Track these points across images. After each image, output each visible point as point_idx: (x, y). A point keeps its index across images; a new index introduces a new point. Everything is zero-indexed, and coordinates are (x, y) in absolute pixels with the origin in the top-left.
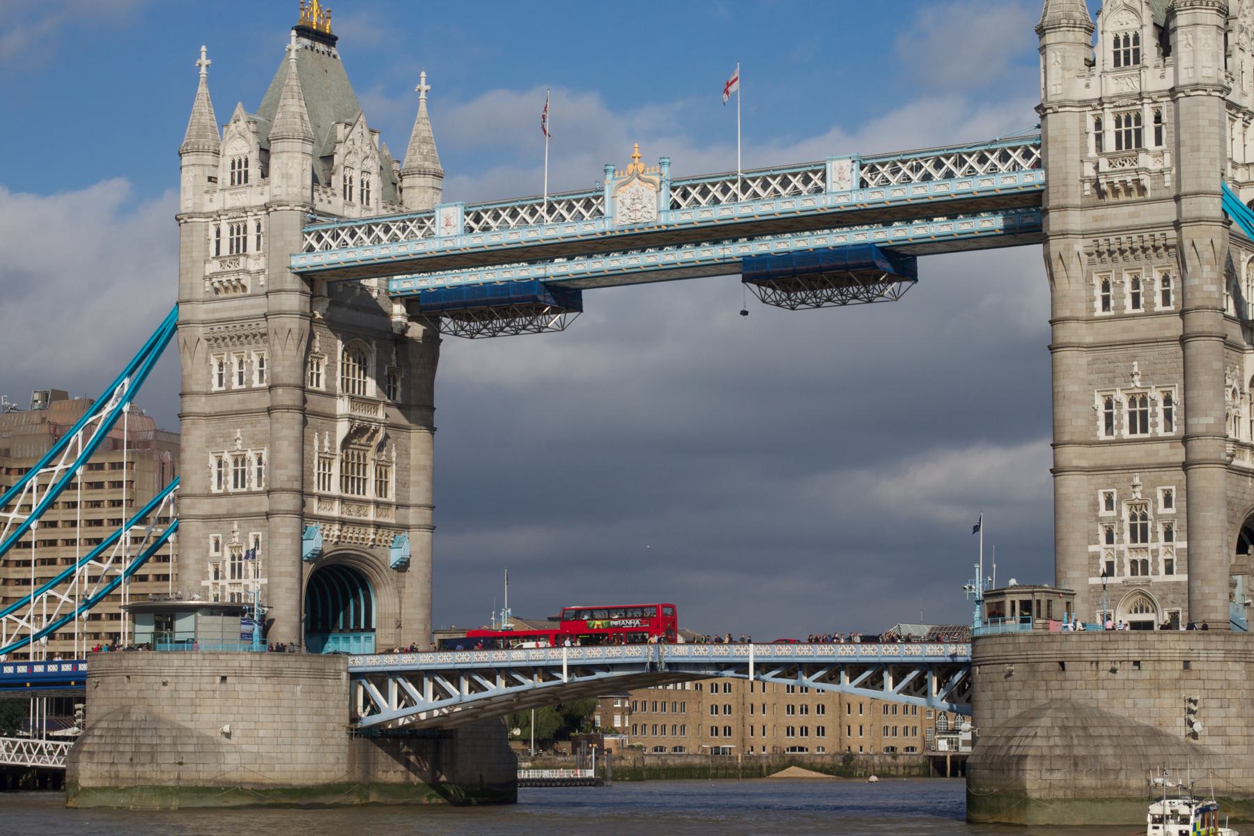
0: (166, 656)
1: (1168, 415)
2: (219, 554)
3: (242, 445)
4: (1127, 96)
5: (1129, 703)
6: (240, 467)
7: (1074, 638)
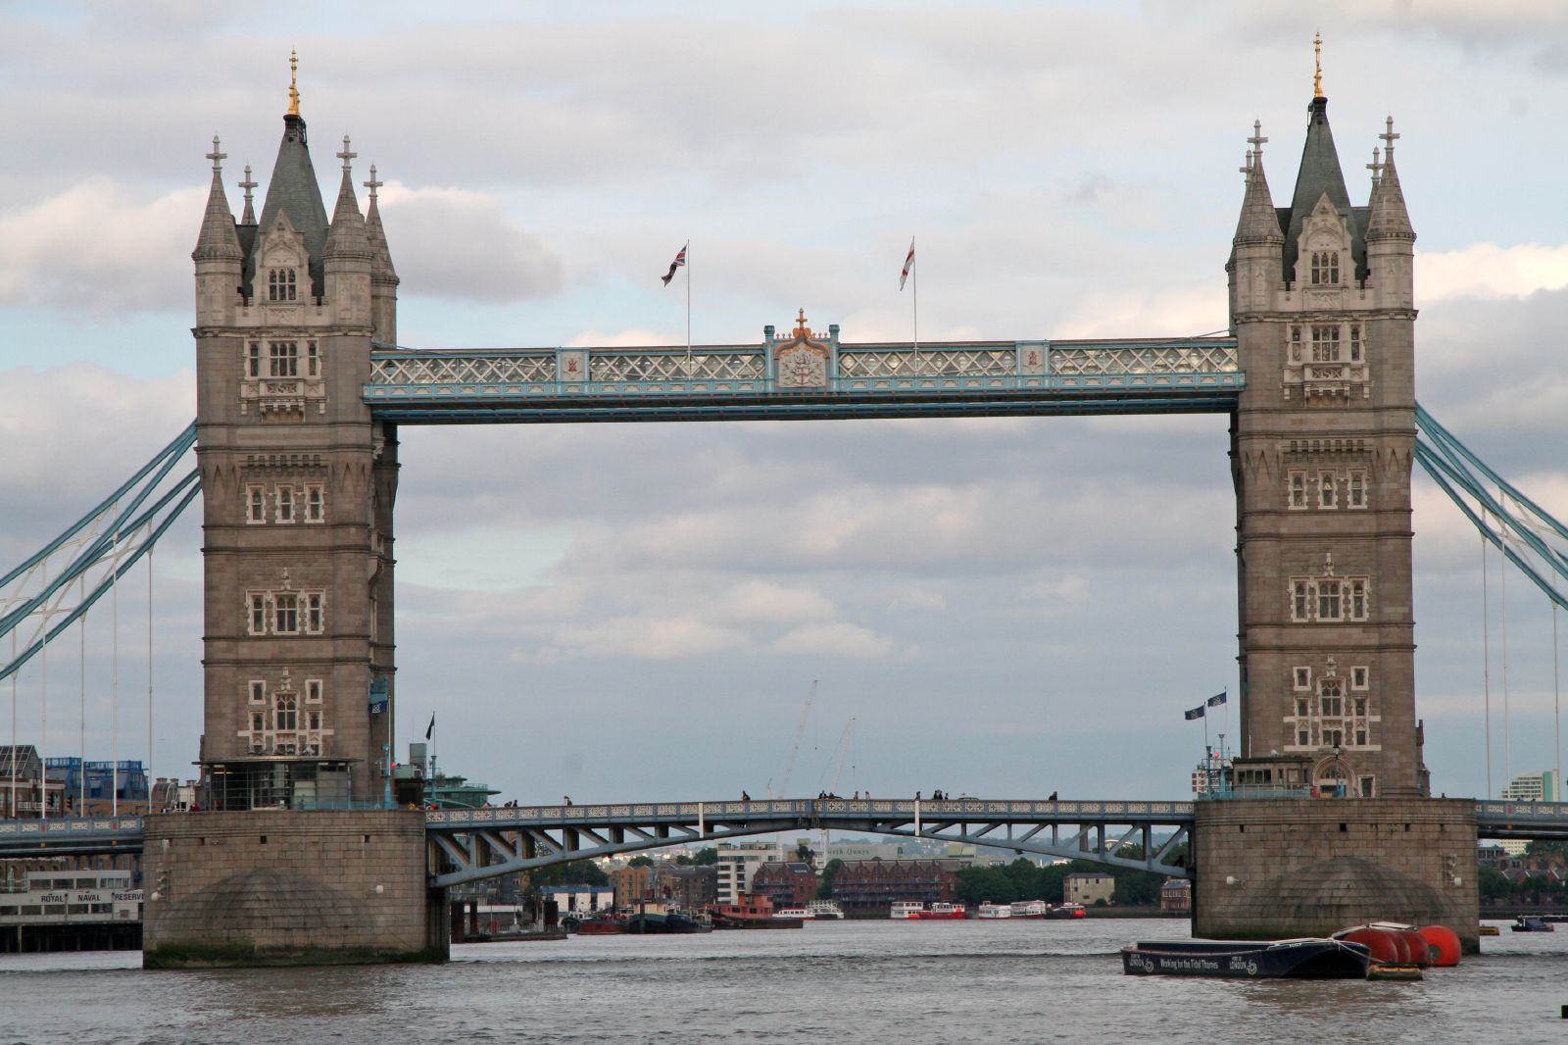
0: (312, 815)
1: (1358, 600)
2: (263, 702)
3: (291, 585)
4: (1330, 312)
5: (1403, 860)
6: (287, 609)
7: (1355, 804)
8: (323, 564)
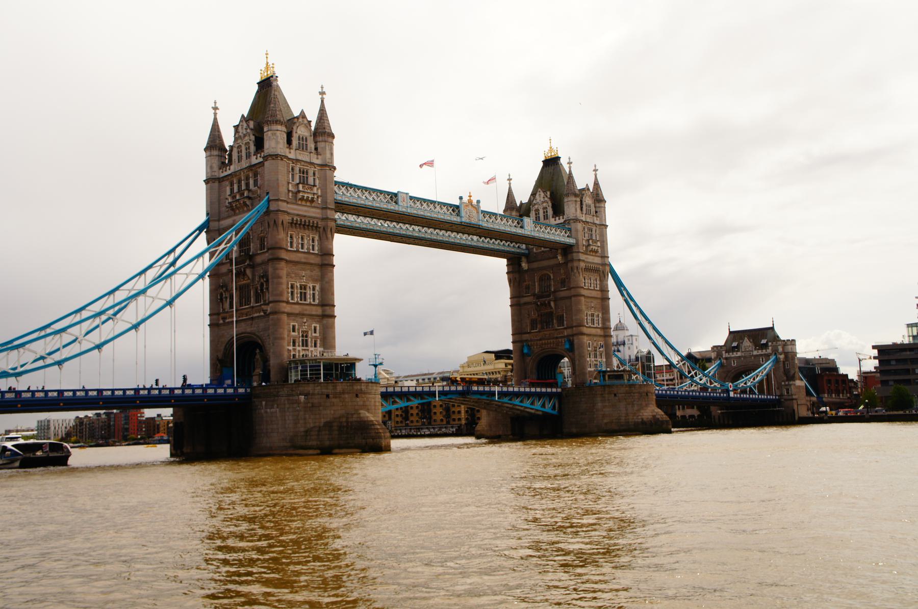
0: (372, 385)
2: (297, 334)
6: (303, 291)
8: (317, 272)
